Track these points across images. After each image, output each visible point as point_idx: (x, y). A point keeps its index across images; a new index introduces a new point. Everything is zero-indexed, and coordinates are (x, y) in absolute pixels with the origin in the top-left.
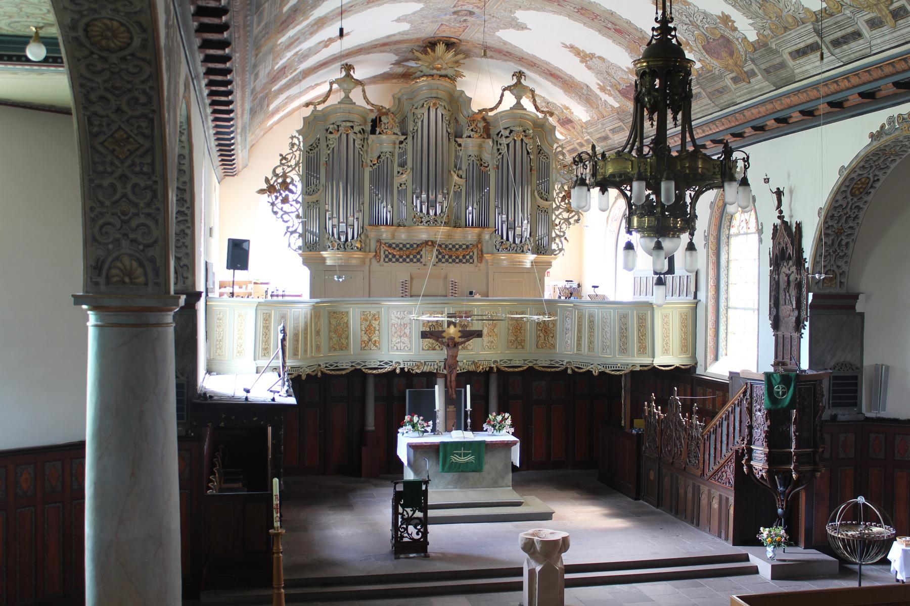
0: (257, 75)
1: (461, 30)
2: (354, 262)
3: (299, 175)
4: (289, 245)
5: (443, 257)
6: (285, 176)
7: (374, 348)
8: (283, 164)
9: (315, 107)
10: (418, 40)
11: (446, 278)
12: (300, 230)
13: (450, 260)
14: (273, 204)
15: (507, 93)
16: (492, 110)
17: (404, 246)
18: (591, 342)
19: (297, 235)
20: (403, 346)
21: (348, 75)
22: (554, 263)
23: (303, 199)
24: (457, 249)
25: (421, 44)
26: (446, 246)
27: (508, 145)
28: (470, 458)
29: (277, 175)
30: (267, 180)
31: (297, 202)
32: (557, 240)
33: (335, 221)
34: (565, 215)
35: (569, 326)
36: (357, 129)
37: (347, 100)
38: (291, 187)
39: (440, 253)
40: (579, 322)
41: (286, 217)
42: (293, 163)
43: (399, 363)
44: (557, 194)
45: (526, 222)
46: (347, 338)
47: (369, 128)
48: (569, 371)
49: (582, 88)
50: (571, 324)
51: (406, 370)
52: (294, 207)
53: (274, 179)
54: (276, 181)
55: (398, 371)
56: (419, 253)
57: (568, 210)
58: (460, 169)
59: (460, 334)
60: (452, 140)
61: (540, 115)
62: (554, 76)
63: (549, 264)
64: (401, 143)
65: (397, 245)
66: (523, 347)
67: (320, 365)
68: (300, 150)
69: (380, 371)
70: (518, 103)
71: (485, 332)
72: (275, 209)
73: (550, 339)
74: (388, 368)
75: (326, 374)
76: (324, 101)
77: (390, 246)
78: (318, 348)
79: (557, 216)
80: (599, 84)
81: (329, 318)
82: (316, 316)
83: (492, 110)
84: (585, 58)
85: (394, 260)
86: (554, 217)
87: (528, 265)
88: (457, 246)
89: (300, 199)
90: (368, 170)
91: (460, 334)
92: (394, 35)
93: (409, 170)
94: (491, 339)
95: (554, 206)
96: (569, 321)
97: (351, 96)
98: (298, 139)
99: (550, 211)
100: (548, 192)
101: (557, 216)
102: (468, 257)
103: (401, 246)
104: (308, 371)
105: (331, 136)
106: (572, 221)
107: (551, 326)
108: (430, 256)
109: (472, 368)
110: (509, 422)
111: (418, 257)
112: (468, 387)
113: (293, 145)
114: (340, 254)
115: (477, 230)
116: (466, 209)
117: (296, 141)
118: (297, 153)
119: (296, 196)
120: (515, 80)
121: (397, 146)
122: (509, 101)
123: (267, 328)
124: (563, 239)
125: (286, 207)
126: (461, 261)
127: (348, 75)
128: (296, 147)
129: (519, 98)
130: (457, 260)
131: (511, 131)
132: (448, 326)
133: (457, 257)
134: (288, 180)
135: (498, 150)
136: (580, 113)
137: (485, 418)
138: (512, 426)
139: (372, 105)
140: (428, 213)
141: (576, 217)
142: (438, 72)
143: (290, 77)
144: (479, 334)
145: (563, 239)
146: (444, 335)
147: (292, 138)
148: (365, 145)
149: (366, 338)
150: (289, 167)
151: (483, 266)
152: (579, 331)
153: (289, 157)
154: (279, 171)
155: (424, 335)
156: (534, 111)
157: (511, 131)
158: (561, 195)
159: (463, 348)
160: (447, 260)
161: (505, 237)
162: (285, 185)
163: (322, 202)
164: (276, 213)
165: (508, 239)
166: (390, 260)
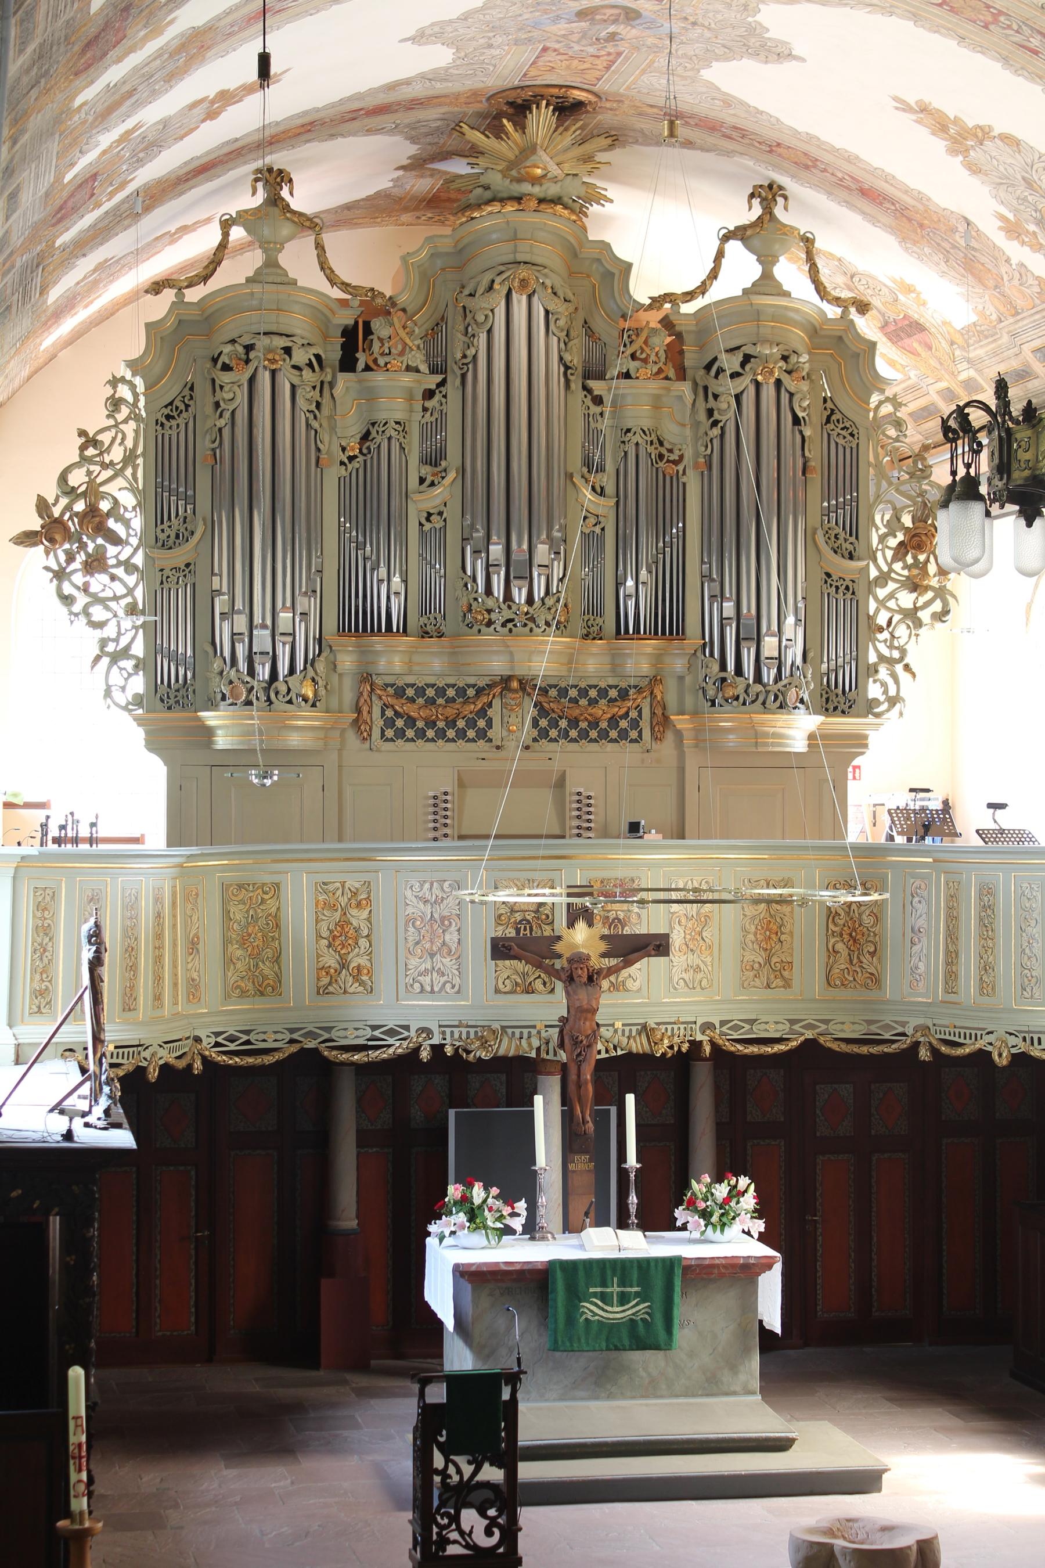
0: (13, 197)
1: (601, 64)
2: (295, 740)
3: (133, 490)
4: (108, 693)
5: (554, 724)
6: (93, 493)
7: (355, 987)
8: (89, 460)
9: (180, 294)
10: (475, 94)
11: (561, 783)
12: (138, 649)
14: (60, 575)
15: (734, 247)
16: (690, 296)
17: (441, 692)
18: (986, 968)
19: (128, 664)
20: (438, 981)
21: (275, 201)
22: (874, 738)
23: (146, 556)
25: (483, 106)
27: (738, 397)
28: (635, 1309)
29: (71, 492)
30: (43, 506)
31: (128, 566)
32: (883, 673)
33: (241, 623)
34: (906, 599)
35: (921, 922)
36: (300, 357)
37: (270, 271)
38: (111, 523)
39: (543, 712)
40: (949, 908)
41: (98, 613)
42: (116, 455)
43: (428, 1032)
44: (882, 539)
45: (790, 620)
46: (277, 959)
47: (333, 353)
48: (924, 1054)
49: (954, 230)
50: (928, 915)
51: (449, 1051)
52: (123, 585)
53: (64, 501)
54: (68, 507)
55: (425, 1055)
56: (482, 713)
57: (914, 586)
58: (601, 469)
59: (603, 947)
60: (576, 385)
61: (833, 312)
62: (869, 194)
63: (859, 742)
64: (429, 394)
65: (421, 691)
66: (787, 984)
67: (198, 1040)
68: (137, 418)
69: (373, 1055)
70: (767, 276)
71: (677, 940)
72: (67, 589)
73: (866, 959)
74: (397, 1047)
75: (216, 1064)
76: (205, 279)
77: (400, 692)
78: (194, 989)
79: (882, 603)
80: (1002, 218)
81: (224, 902)
82: (186, 898)
83: (690, 296)
84: (963, 139)
86: (872, 606)
87: (799, 745)
88: (593, 693)
89: (139, 560)
90: (333, 474)
91: (603, 947)
92: (407, 82)
93: (452, 475)
94: (694, 960)
95: (873, 573)
96: (922, 908)
97: (283, 259)
98: (133, 387)
99: (861, 589)
100: (854, 531)
101: (882, 603)
103: (430, 692)
104: (166, 1056)
105: (225, 378)
106: (924, 615)
107: (867, 920)
109: (639, 1045)
110: (749, 1201)
111: (481, 723)
112: (630, 1099)
113: (115, 403)
114: (255, 718)
115: (650, 646)
116: (619, 584)
117: (123, 391)
118: (130, 428)
119: (127, 551)
120: (757, 211)
121: (418, 406)
122: (741, 269)
123: (45, 930)
124: (899, 668)
125: (98, 582)
126: (604, 735)
127: (275, 201)
128: (125, 411)
129: (767, 261)
130: (593, 734)
131: (747, 359)
132: (571, 924)
133: (594, 724)
134: (105, 506)
135: (710, 412)
136: (946, 301)
137: (677, 1191)
138: (759, 1213)
139: (345, 286)
140: (508, 597)
141: (937, 606)
142: (536, 190)
143: (107, 206)
144: (657, 945)
145: (899, 668)
146: (559, 947)
147: (114, 382)
148: (326, 401)
149: (331, 960)
150: (105, 466)
151: (667, 748)
152: (952, 935)
153: (106, 438)
154: (77, 478)
155: (500, 950)
156: (815, 298)
157: (747, 359)
158: (893, 542)
159: (615, 987)
160: (565, 735)
161: (731, 665)
162: (94, 520)
163: (202, 568)
164: (67, 600)
165: (739, 671)
166: (400, 734)
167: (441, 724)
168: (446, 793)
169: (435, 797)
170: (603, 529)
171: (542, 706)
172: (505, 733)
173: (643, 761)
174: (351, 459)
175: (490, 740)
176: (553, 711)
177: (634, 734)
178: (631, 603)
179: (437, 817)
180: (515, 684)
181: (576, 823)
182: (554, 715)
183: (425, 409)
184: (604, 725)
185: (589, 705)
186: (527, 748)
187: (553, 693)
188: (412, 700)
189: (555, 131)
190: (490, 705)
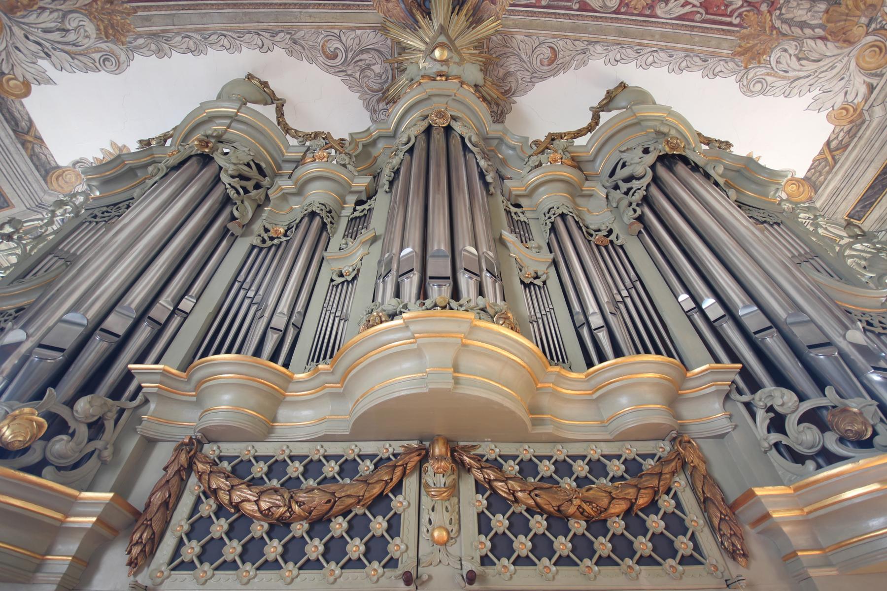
5: (519, 525)
13: (563, 545)
16: (579, 133)
17: (312, 467)
24: (581, 482)
26: (528, 468)
39: (496, 503)
56: (380, 504)
65: (276, 467)
77: (240, 470)
102: (656, 524)
103: (295, 469)
108: (439, 525)
133: (598, 525)
167: (299, 528)
170: (544, 283)
171: (494, 492)
174: (272, 239)
175: (392, 563)
176: (517, 500)
177: (683, 545)
178: (603, 336)
180: (439, 450)
182: (520, 509)
183: (355, 210)
184: (617, 526)
185: (578, 486)
186: (471, 578)
187: (512, 468)
188: (253, 483)
189: (453, 12)
190: (398, 489)
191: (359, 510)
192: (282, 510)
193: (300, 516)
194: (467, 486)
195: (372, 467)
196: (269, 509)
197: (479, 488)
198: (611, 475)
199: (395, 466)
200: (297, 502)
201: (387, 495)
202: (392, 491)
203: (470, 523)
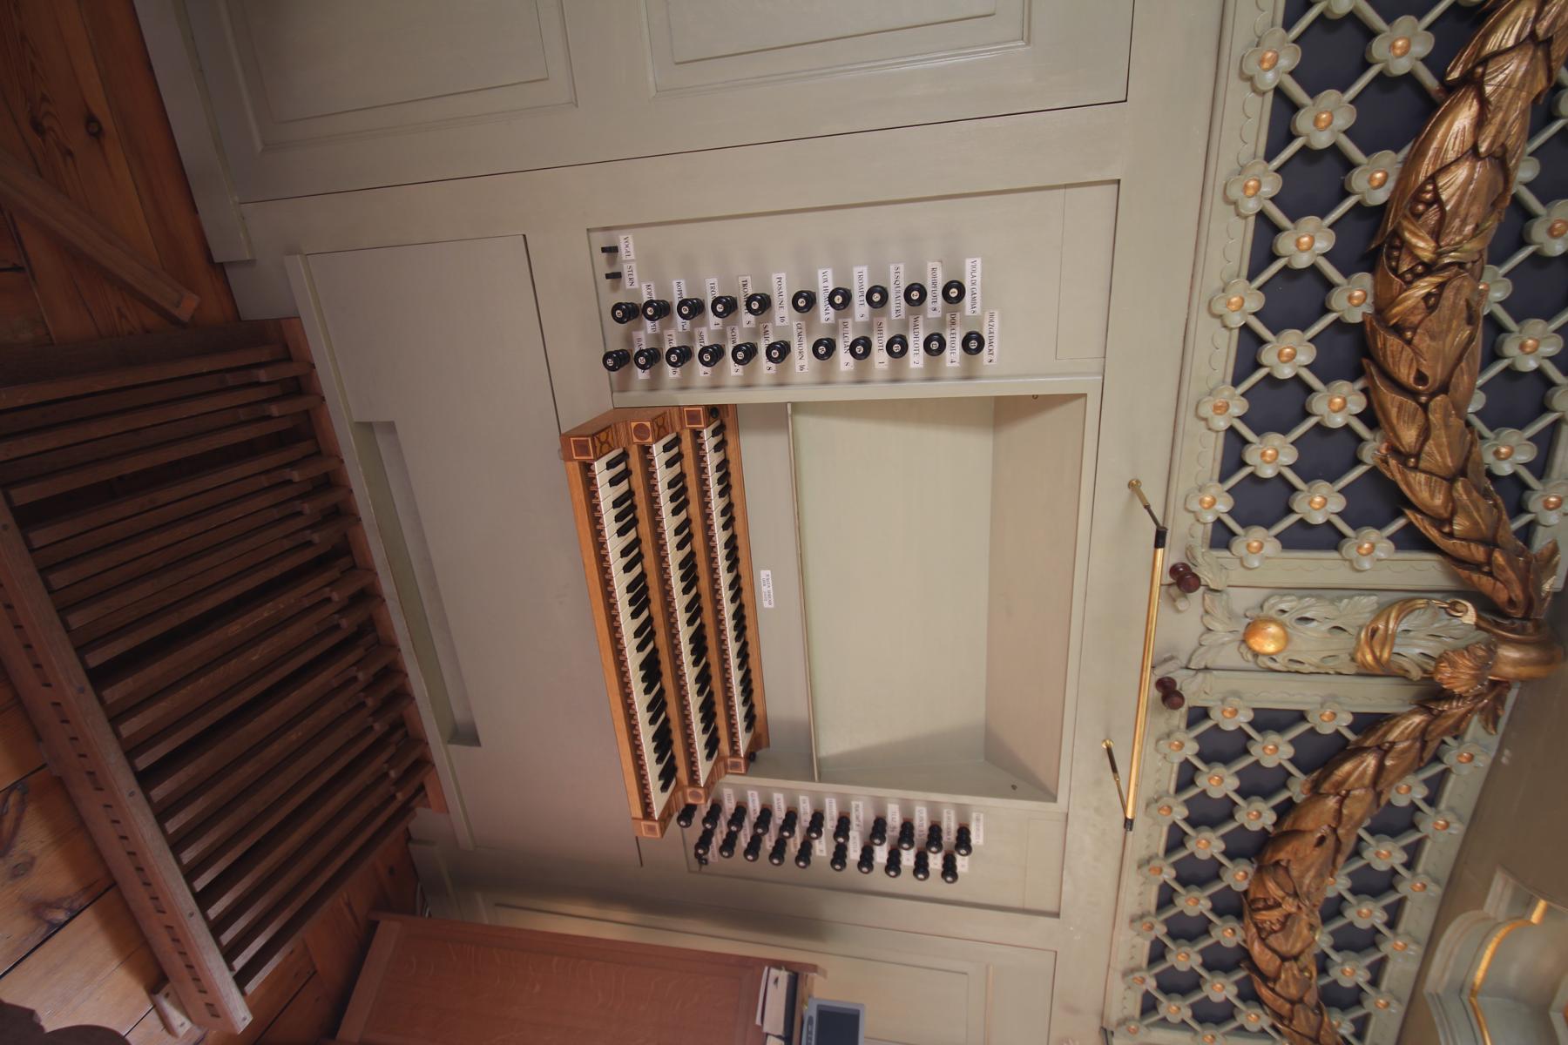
24: (1333, 909)
39: (1321, 756)
56: (1380, 501)
85: (1327, 120)
133: (1234, 907)
168: (973, 343)
169: (954, 292)
172: (1243, 600)
173: (1072, 1010)
175: (1222, 537)
179: (860, 309)
181: (861, 817)
184: (1227, 934)
186: (1168, 692)
190: (1411, 540)
191: (1373, 449)
192: (1424, 246)
193: (1393, 302)
194: (1377, 696)
195: (1505, 469)
196: (1437, 199)
197: (1368, 723)
198: (1335, 956)
199: (1491, 543)
200: (1441, 286)
201: (1401, 514)
202: (1410, 525)
203: (1280, 694)
